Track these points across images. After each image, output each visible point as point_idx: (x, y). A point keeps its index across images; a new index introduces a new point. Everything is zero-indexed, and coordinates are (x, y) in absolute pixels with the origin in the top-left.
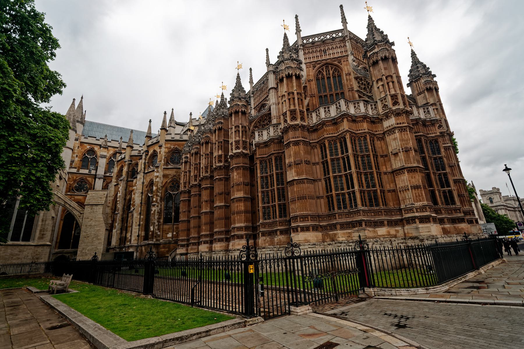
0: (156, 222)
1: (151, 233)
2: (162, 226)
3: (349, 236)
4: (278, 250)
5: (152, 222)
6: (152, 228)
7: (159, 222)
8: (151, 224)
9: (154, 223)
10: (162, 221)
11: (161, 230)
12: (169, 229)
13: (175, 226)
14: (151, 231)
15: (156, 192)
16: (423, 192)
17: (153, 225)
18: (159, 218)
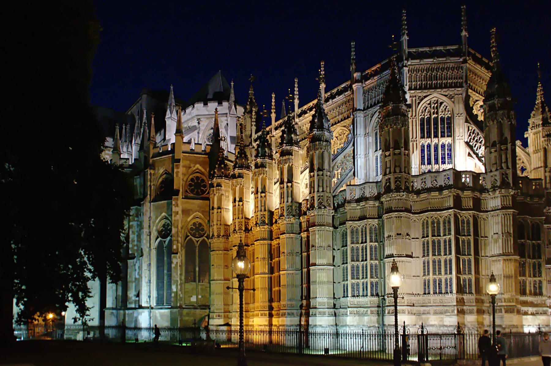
0: (179, 279)
1: (173, 295)
2: (183, 286)
3: (441, 321)
4: (369, 330)
5: (175, 279)
6: (174, 288)
7: (181, 280)
8: (172, 282)
9: (177, 281)
10: (183, 278)
11: (183, 291)
12: (193, 290)
13: (200, 287)
14: (174, 292)
15: (176, 236)
16: (514, 284)
17: (176, 284)
18: (181, 275)
